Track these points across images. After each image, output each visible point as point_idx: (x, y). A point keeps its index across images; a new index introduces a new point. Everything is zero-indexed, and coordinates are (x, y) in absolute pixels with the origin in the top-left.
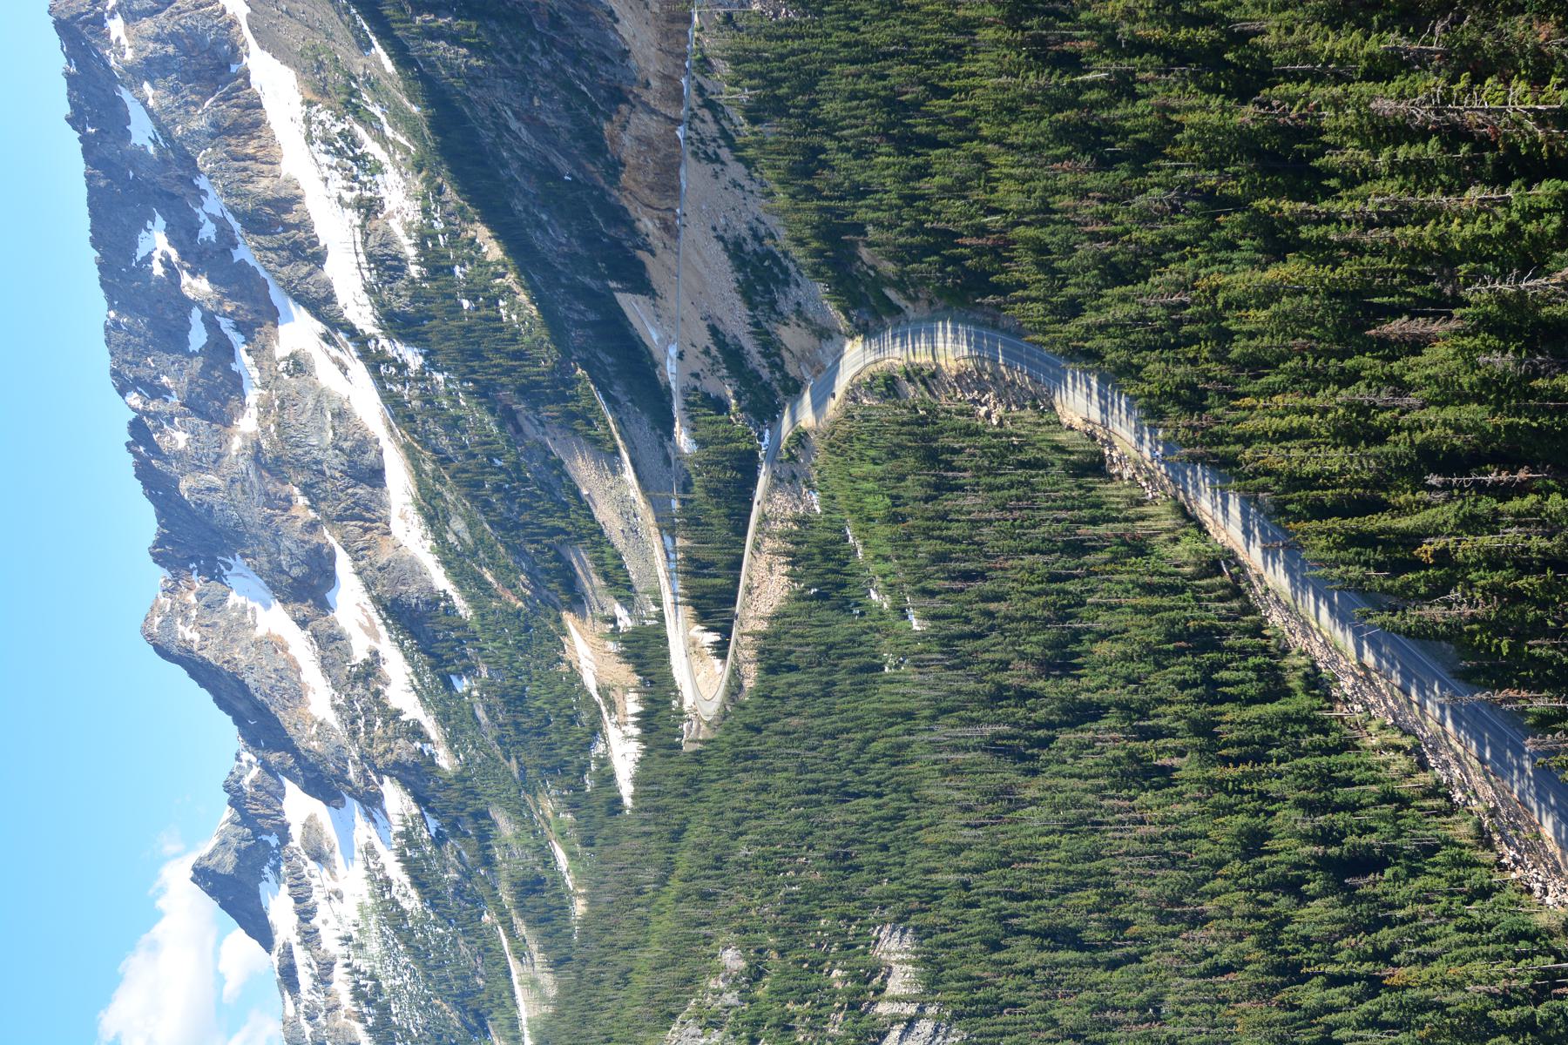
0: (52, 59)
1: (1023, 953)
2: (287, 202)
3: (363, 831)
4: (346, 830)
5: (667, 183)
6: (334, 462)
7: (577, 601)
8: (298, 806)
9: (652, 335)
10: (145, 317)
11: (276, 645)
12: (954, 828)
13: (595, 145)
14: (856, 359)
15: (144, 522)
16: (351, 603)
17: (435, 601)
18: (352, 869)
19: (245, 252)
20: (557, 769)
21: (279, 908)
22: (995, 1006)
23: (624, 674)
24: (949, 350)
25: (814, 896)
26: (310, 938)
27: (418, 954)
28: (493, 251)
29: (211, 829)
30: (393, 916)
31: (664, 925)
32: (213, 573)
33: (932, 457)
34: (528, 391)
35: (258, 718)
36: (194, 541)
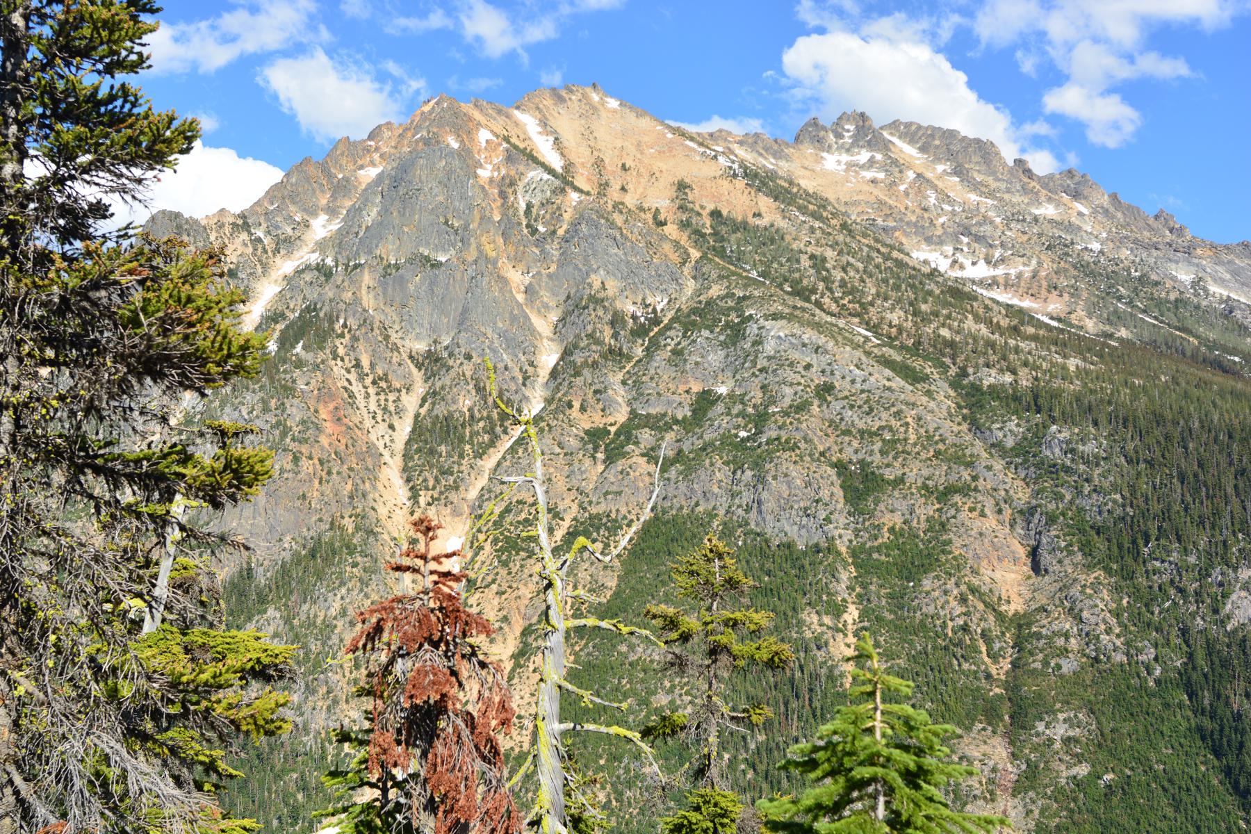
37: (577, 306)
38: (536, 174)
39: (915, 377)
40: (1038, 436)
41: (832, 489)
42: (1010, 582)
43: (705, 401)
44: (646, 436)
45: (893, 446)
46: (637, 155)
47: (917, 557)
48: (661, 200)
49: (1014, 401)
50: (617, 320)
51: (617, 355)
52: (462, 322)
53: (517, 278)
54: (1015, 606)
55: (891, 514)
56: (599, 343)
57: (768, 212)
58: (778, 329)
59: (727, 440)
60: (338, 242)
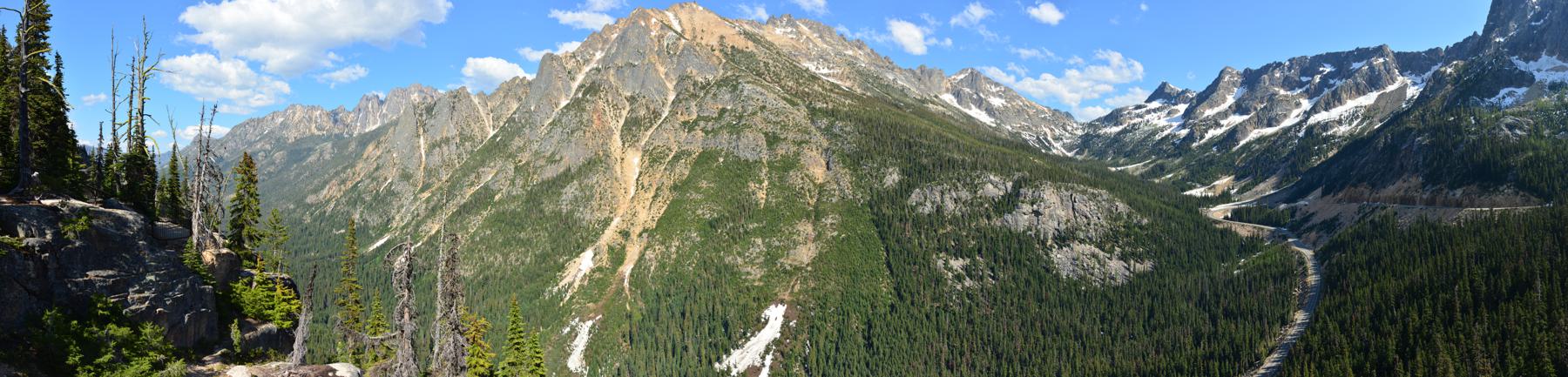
0: (1373, 45)
1: (1147, 301)
2: (1341, 102)
3: (1175, 124)
4: (1176, 120)
5: (1351, 200)
6: (1273, 114)
7: (1237, 179)
8: (1182, 108)
9: (1310, 197)
10: (1309, 66)
11: (1224, 100)
12: (1180, 282)
13: (1361, 181)
14: (1308, 253)
15: (1255, 66)
16: (1236, 119)
17: (1237, 142)
18: (1164, 122)
19: (1326, 91)
20: (1193, 174)
21: (1155, 104)
22: (1133, 293)
23: (1219, 192)
24: (1312, 279)
25: (1161, 244)
26: (1148, 112)
27: (1144, 140)
28: (1330, 154)
29: (1175, 86)
30: (1154, 132)
31: (1153, 204)
32: (1242, 84)
33: (1283, 276)
34: (1294, 165)
35: (1205, 97)
36: (1251, 79)
37: (682, 79)
38: (671, 33)
39: (794, 104)
40: (832, 125)
41: (763, 142)
42: (819, 173)
43: (723, 111)
44: (702, 124)
45: (784, 127)
46: (706, 27)
47: (790, 164)
48: (714, 42)
49: (826, 113)
50: (695, 84)
51: (694, 96)
52: (643, 86)
53: (662, 70)
54: (821, 181)
55: (781, 150)
56: (689, 91)
57: (751, 46)
58: (749, 87)
59: (729, 125)
60: (603, 60)
